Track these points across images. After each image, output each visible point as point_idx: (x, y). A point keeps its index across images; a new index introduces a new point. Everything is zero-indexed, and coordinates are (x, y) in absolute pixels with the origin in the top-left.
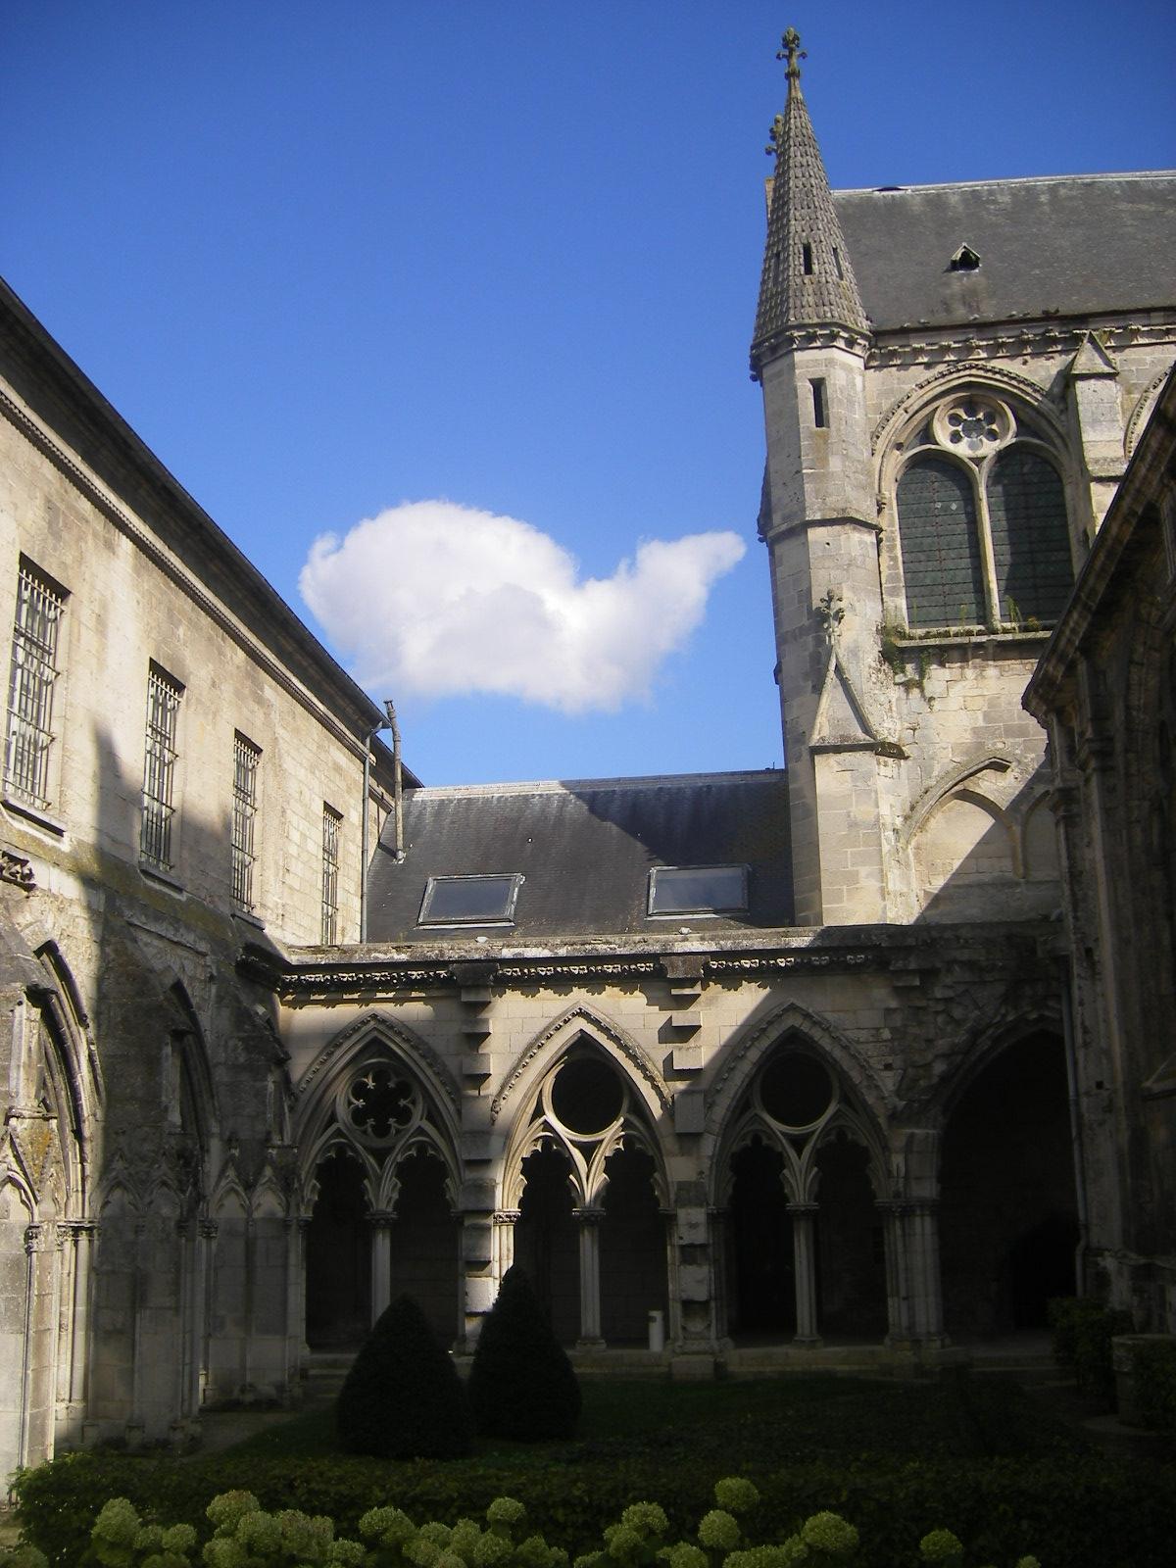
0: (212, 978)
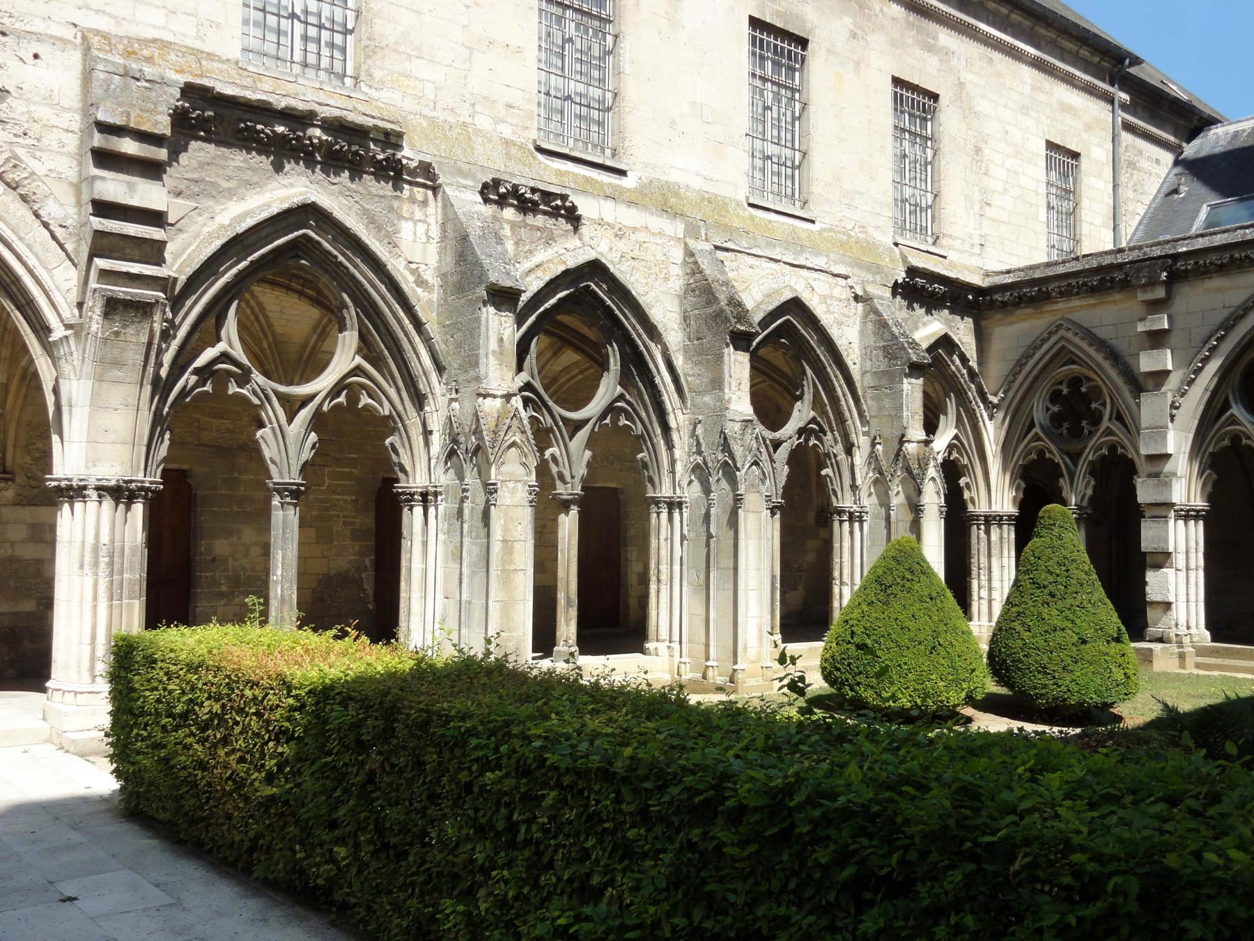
0: (857, 298)
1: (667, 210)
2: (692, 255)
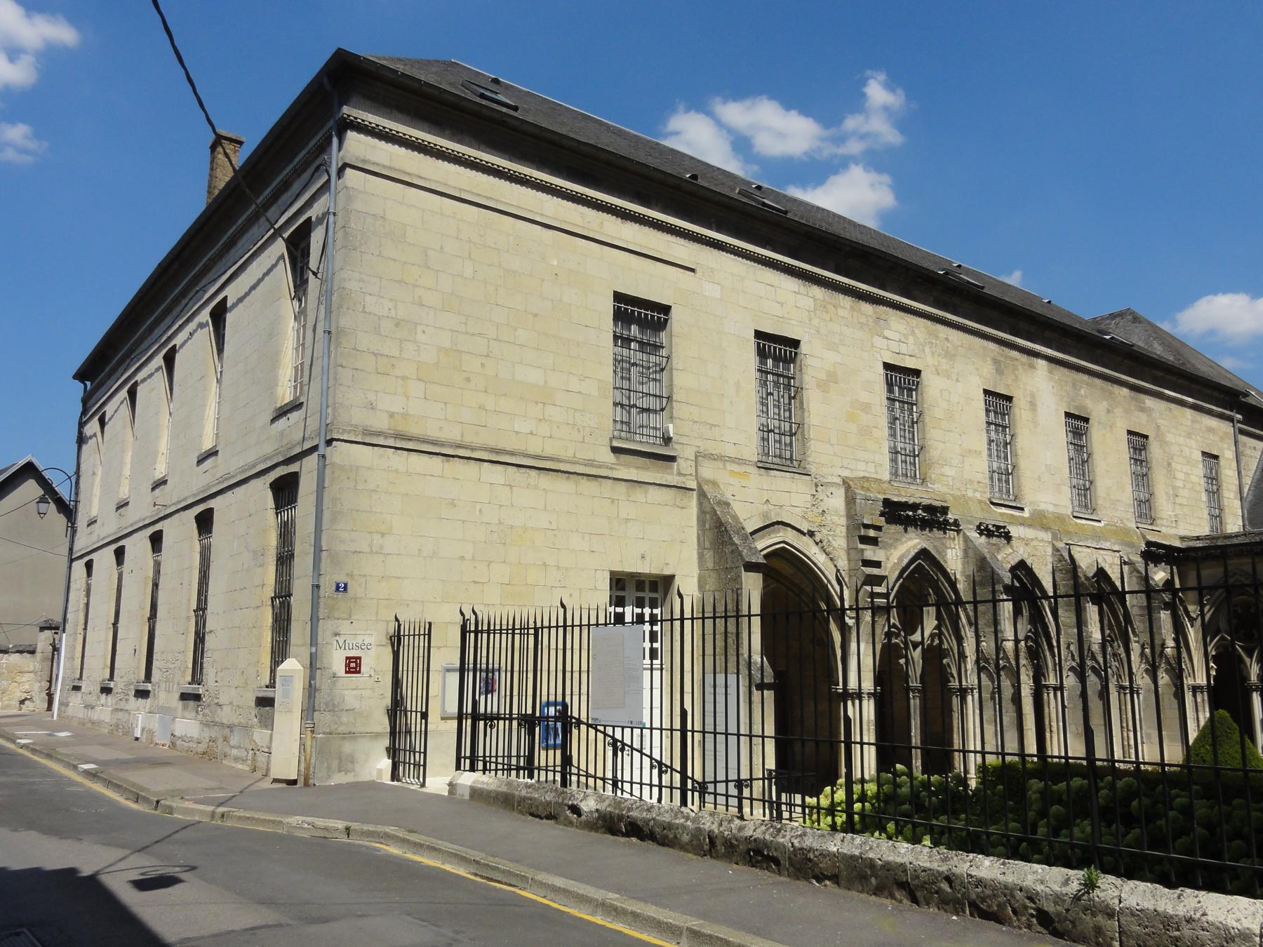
1: (1045, 528)
2: (1058, 550)
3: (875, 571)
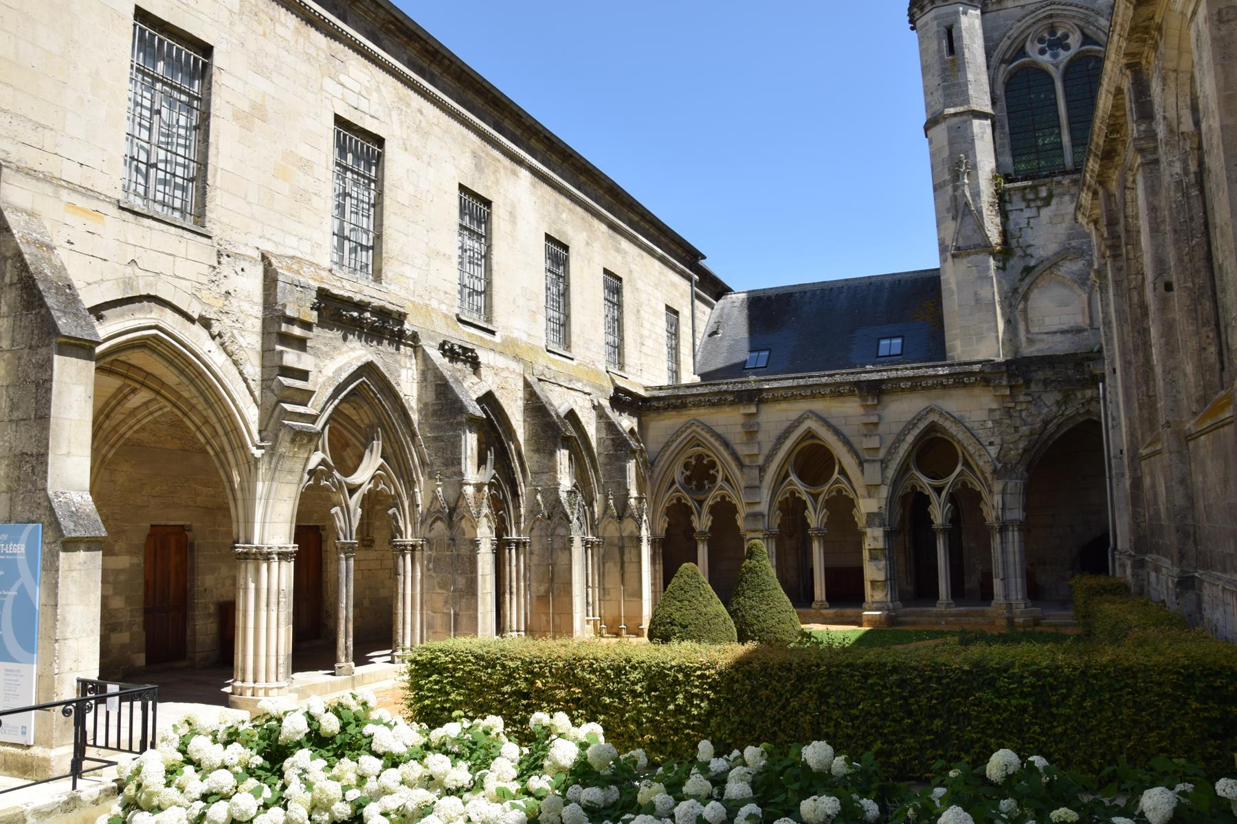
1: (516, 358)
3: (298, 384)
